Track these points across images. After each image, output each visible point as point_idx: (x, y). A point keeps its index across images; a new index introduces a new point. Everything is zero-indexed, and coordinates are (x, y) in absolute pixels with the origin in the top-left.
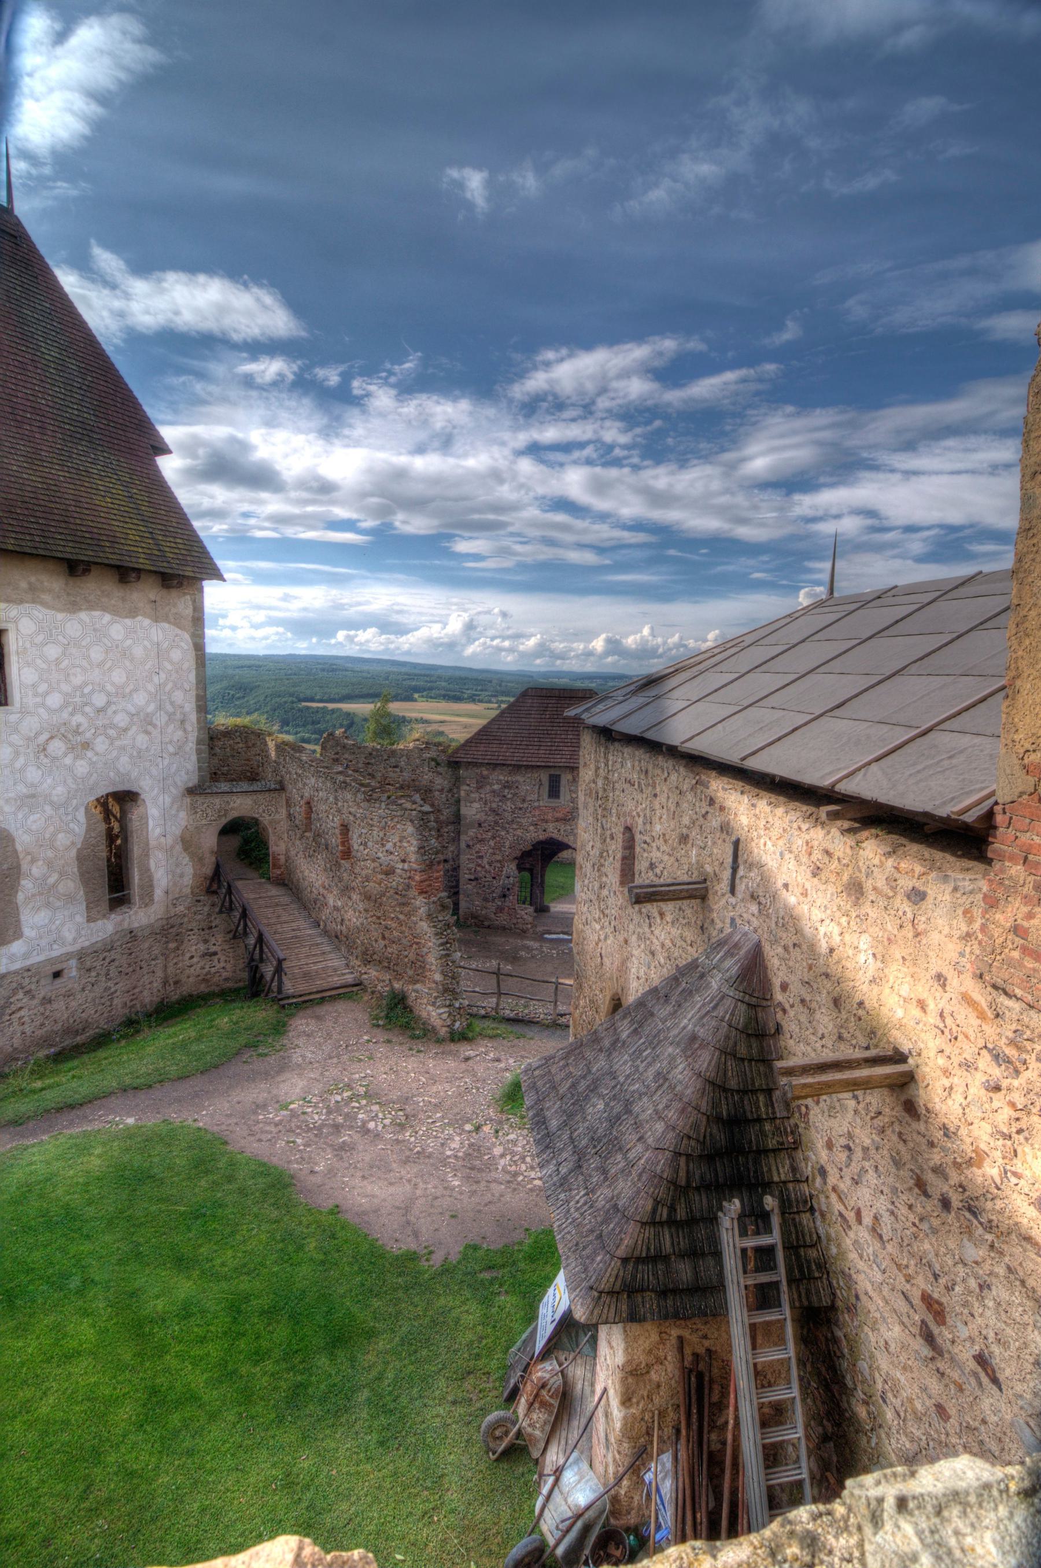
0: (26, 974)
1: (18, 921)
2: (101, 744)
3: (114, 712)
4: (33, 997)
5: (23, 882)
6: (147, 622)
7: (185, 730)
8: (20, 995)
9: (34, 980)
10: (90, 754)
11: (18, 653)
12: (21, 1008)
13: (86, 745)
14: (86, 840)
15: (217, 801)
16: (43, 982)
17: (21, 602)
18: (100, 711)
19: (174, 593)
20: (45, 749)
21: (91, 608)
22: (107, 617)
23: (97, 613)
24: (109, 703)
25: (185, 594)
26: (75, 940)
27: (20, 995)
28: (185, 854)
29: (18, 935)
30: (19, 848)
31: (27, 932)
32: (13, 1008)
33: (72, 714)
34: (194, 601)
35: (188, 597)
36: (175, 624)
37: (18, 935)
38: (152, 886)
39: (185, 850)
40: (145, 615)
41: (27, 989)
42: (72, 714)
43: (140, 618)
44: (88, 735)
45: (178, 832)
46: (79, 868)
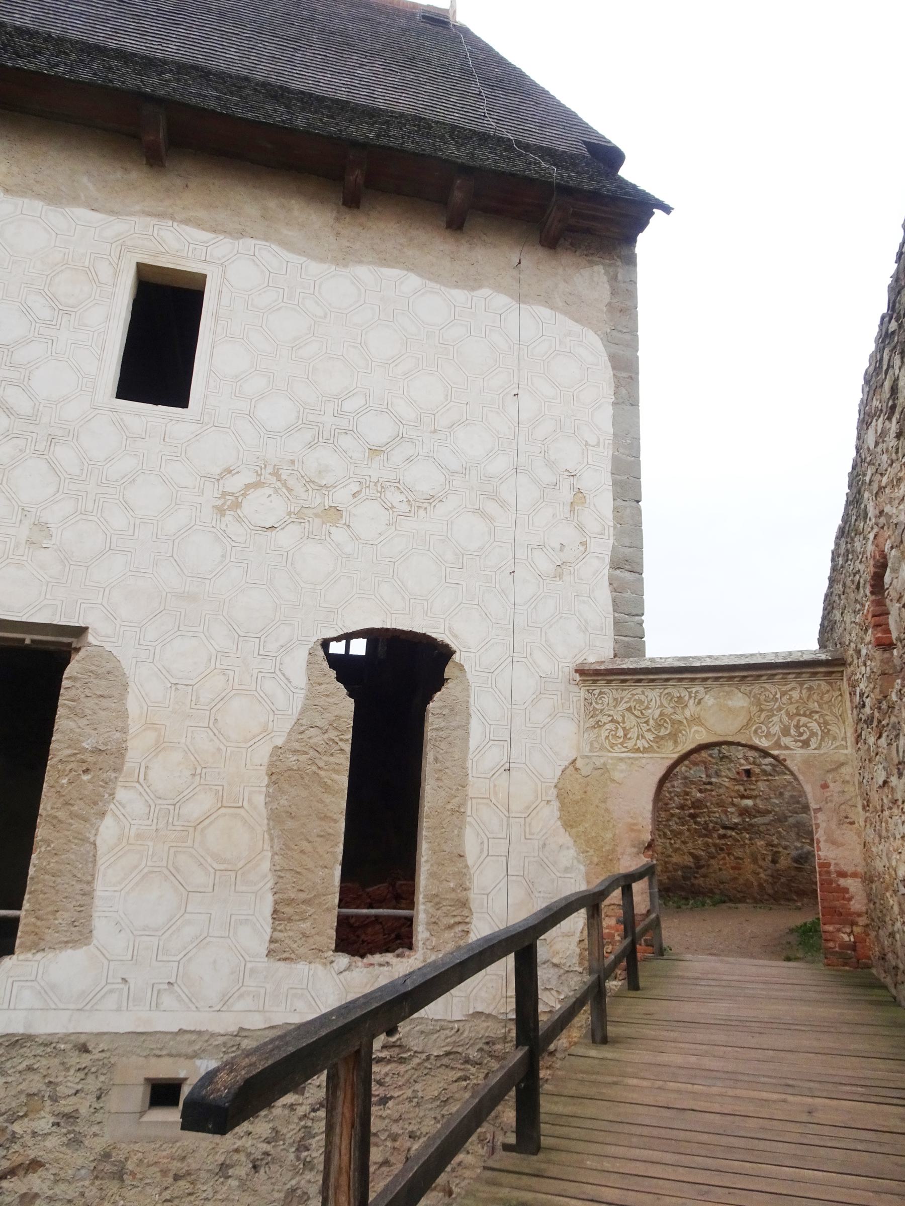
0: (75, 1059)
1: (88, 894)
2: (368, 517)
3: (409, 460)
4: (76, 1142)
5: (121, 794)
6: (501, 300)
7: (580, 527)
8: (44, 1123)
9: (92, 1084)
10: (339, 534)
11: (216, 316)
12: (35, 1165)
13: (333, 514)
14: (299, 729)
15: (652, 697)
16: (113, 1102)
17: (242, 234)
18: (374, 451)
19: (567, 258)
20: (237, 505)
21: (384, 262)
22: (413, 281)
23: (392, 273)
24: (399, 438)
25: (592, 263)
26: (226, 1001)
27: (44, 1123)
28: (565, 838)
29: (80, 933)
30: (133, 705)
31: (101, 927)
32: (18, 1154)
33: (310, 446)
34: (614, 279)
35: (599, 269)
36: (565, 313)
37: (80, 933)
38: (464, 903)
39: (569, 824)
40: (498, 288)
41: (66, 1106)
42: (310, 446)
43: (485, 292)
44: (341, 497)
45: (552, 773)
46: (270, 798)
